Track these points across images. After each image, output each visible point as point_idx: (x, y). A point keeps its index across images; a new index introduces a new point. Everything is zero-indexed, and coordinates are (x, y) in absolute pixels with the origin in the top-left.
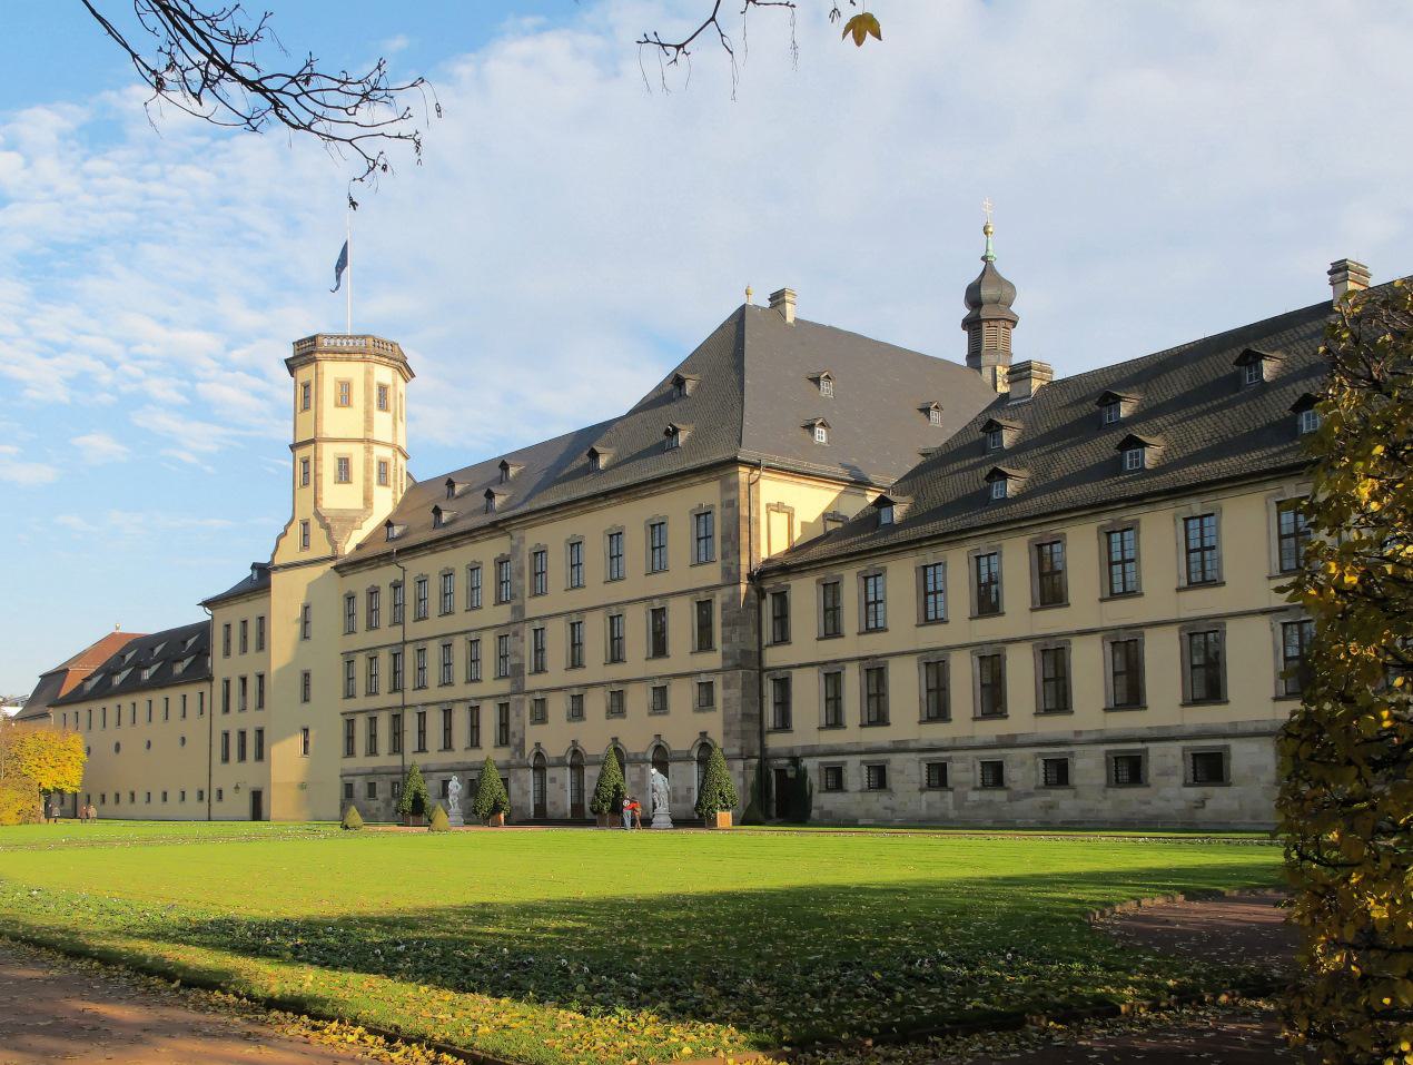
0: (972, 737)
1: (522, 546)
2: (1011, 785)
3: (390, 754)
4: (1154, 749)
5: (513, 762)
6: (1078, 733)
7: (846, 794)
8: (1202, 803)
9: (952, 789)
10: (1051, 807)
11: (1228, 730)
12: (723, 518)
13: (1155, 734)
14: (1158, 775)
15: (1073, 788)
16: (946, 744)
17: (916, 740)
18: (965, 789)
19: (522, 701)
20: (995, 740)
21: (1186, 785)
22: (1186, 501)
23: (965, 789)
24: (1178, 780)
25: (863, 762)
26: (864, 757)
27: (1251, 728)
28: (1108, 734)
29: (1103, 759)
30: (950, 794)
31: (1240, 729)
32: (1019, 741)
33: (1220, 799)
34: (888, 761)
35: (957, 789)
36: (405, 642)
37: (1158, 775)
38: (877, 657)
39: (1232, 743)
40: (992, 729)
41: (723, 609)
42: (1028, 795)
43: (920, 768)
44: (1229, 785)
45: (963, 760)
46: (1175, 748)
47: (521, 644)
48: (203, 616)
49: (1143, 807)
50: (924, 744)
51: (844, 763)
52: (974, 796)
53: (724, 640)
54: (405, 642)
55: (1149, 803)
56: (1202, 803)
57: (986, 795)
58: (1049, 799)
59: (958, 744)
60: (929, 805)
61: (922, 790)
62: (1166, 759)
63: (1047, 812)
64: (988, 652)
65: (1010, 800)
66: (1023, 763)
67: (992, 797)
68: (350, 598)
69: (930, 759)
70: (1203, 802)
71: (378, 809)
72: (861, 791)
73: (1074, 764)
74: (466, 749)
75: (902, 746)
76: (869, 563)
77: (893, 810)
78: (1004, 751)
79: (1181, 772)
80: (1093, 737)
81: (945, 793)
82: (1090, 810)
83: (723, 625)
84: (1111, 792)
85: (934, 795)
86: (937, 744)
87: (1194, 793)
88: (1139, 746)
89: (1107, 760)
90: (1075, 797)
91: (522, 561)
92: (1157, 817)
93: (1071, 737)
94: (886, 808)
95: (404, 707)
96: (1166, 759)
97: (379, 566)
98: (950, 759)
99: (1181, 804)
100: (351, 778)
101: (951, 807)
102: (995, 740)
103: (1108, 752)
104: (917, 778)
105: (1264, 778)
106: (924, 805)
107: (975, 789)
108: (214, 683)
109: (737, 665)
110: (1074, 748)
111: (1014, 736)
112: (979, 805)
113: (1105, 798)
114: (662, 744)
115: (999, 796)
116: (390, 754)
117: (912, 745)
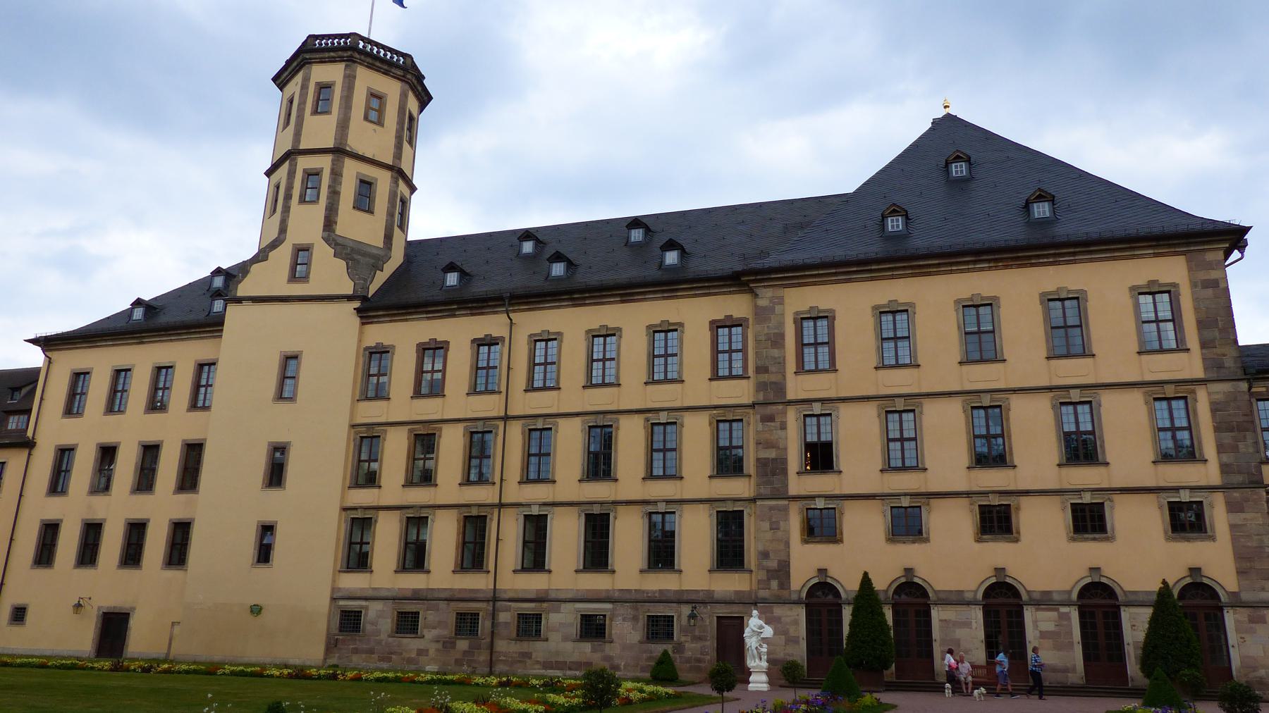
1: (778, 308)
3: (396, 572)
5: (763, 594)
12: (1196, 300)
19: (785, 510)
36: (506, 418)
47: (781, 433)
48: (34, 358)
53: (1220, 449)
54: (506, 418)
68: (379, 353)
71: (421, 652)
74: (641, 571)
83: (1217, 429)
91: (781, 324)
95: (501, 505)
97: (454, 316)
100: (364, 603)
108: (36, 452)
109: (1251, 482)
114: (829, 580)
116: (396, 572)
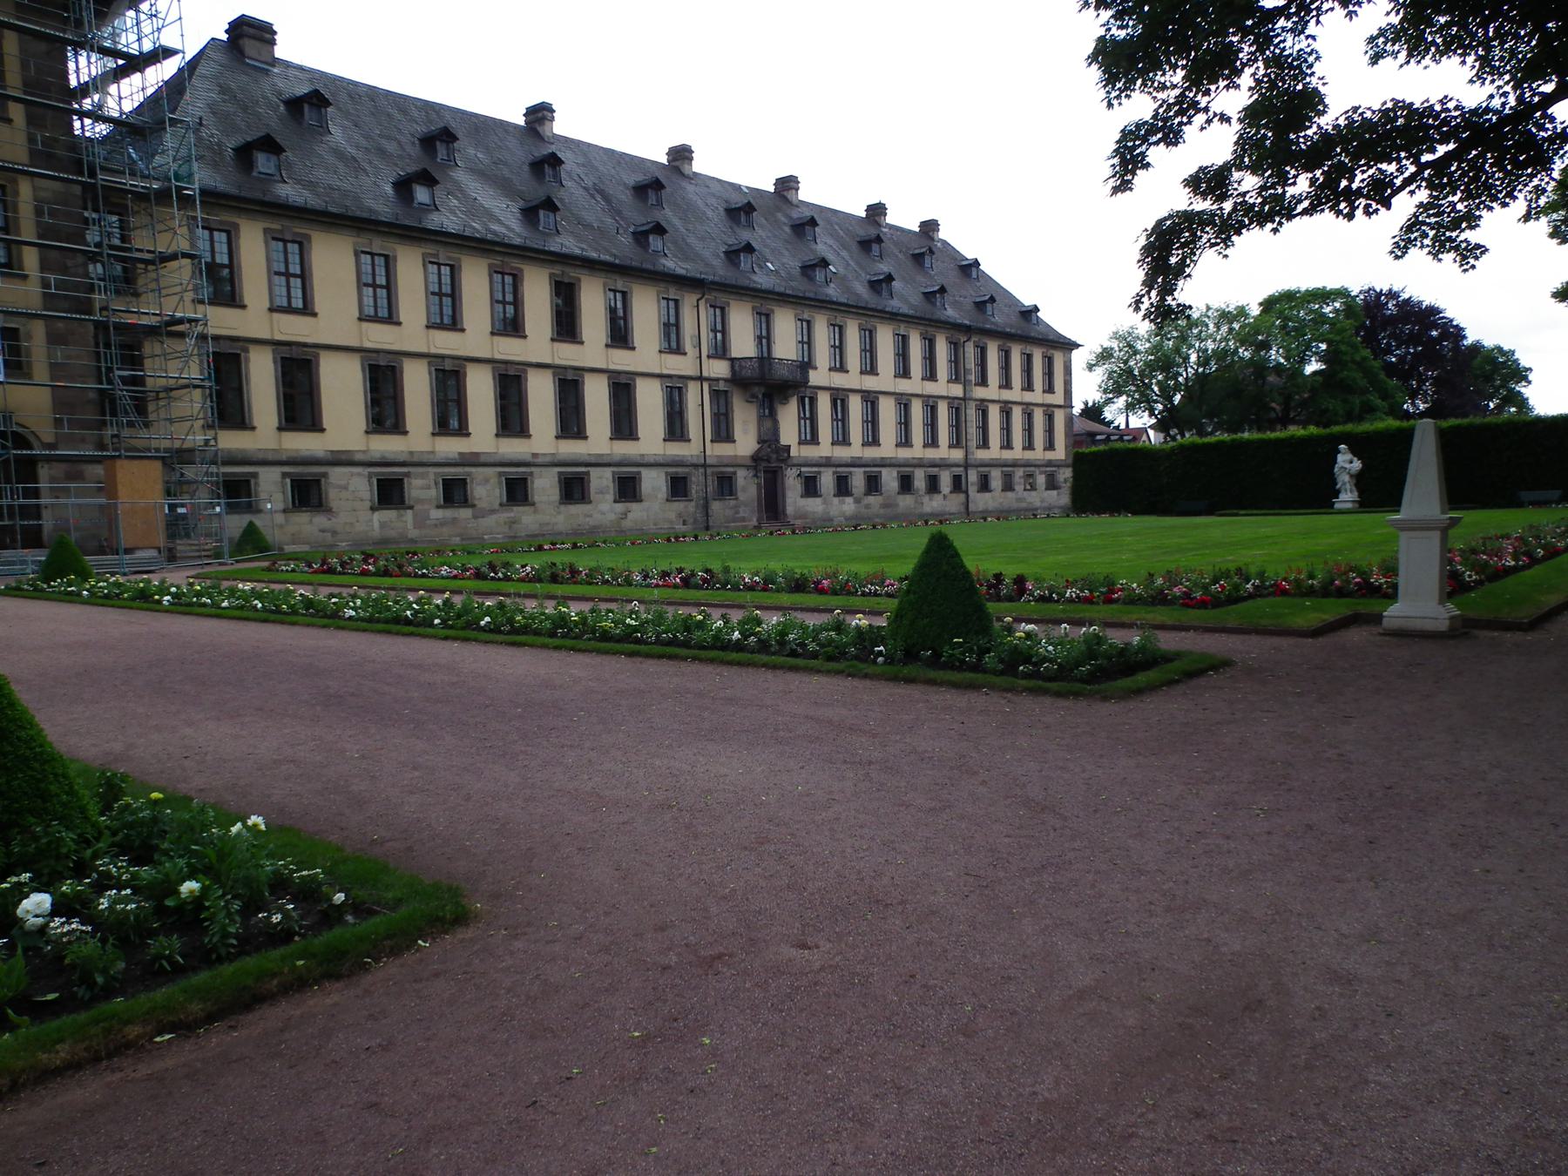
0: (433, 452)
2: (476, 502)
4: (595, 473)
6: (535, 455)
7: (262, 515)
8: (625, 515)
9: (411, 508)
10: (514, 523)
11: (639, 460)
13: (593, 460)
14: (596, 493)
15: (533, 504)
16: (401, 459)
17: (364, 452)
18: (426, 507)
20: (457, 456)
21: (615, 501)
22: (616, 277)
23: (426, 507)
24: (610, 497)
25: (284, 475)
26: (287, 469)
27: (652, 461)
28: (560, 458)
29: (557, 479)
30: (409, 512)
31: (646, 460)
32: (483, 459)
33: (636, 513)
34: (325, 475)
35: (417, 507)
37: (596, 493)
38: (305, 345)
39: (641, 469)
40: (450, 447)
41: (39, 212)
42: (493, 511)
43: (371, 485)
44: (641, 501)
45: (423, 476)
46: (608, 473)
49: (588, 519)
50: (376, 457)
51: (255, 475)
52: (437, 514)
55: (591, 516)
56: (625, 515)
57: (448, 513)
58: (512, 515)
59: (415, 459)
60: (383, 525)
61: (373, 509)
62: (602, 481)
63: (510, 527)
64: (448, 365)
65: (475, 517)
66: (487, 481)
67: (456, 515)
69: (383, 474)
70: (626, 514)
72: (285, 511)
73: (533, 483)
75: (343, 457)
76: (287, 223)
77: (334, 533)
78: (467, 469)
79: (612, 492)
80: (548, 459)
81: (402, 512)
82: (548, 524)
84: (563, 508)
85: (389, 515)
86: (391, 457)
87: (620, 507)
88: (583, 469)
89: (560, 481)
90: (535, 512)
92: (595, 527)
93: (529, 458)
94: (323, 531)
96: (602, 481)
98: (408, 475)
99: (612, 517)
101: (410, 525)
102: (457, 456)
103: (560, 474)
104: (367, 495)
105: (660, 496)
106: (376, 525)
107: (438, 507)
110: (533, 469)
111: (477, 454)
112: (442, 523)
113: (559, 513)
115: (465, 513)
117: (359, 457)
